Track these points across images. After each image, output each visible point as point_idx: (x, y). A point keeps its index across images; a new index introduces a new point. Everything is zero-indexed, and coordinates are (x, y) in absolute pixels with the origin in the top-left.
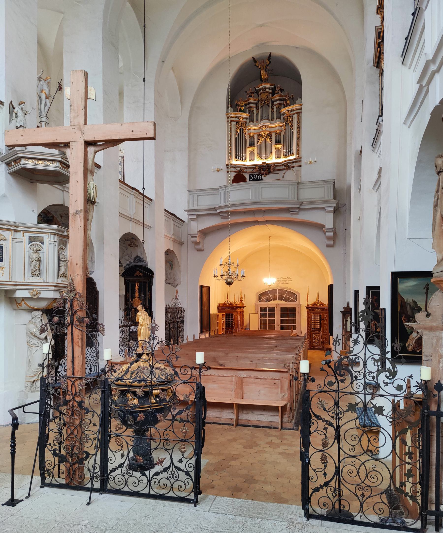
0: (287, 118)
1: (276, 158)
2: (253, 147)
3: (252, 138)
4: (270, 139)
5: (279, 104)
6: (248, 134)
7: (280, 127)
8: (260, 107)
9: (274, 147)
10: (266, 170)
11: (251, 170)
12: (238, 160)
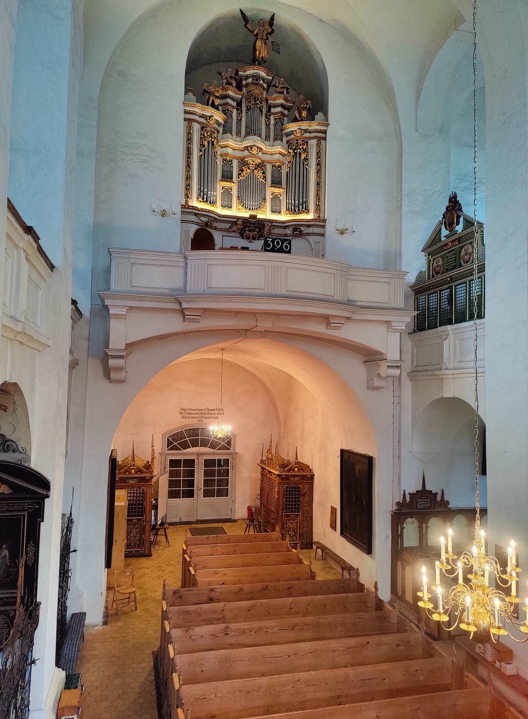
0: (297, 143)
1: (273, 211)
2: (230, 182)
3: (227, 163)
4: (263, 173)
5: (282, 113)
6: (221, 155)
7: (281, 156)
8: (244, 108)
9: (270, 191)
10: (254, 231)
11: (228, 226)
12: (204, 202)
